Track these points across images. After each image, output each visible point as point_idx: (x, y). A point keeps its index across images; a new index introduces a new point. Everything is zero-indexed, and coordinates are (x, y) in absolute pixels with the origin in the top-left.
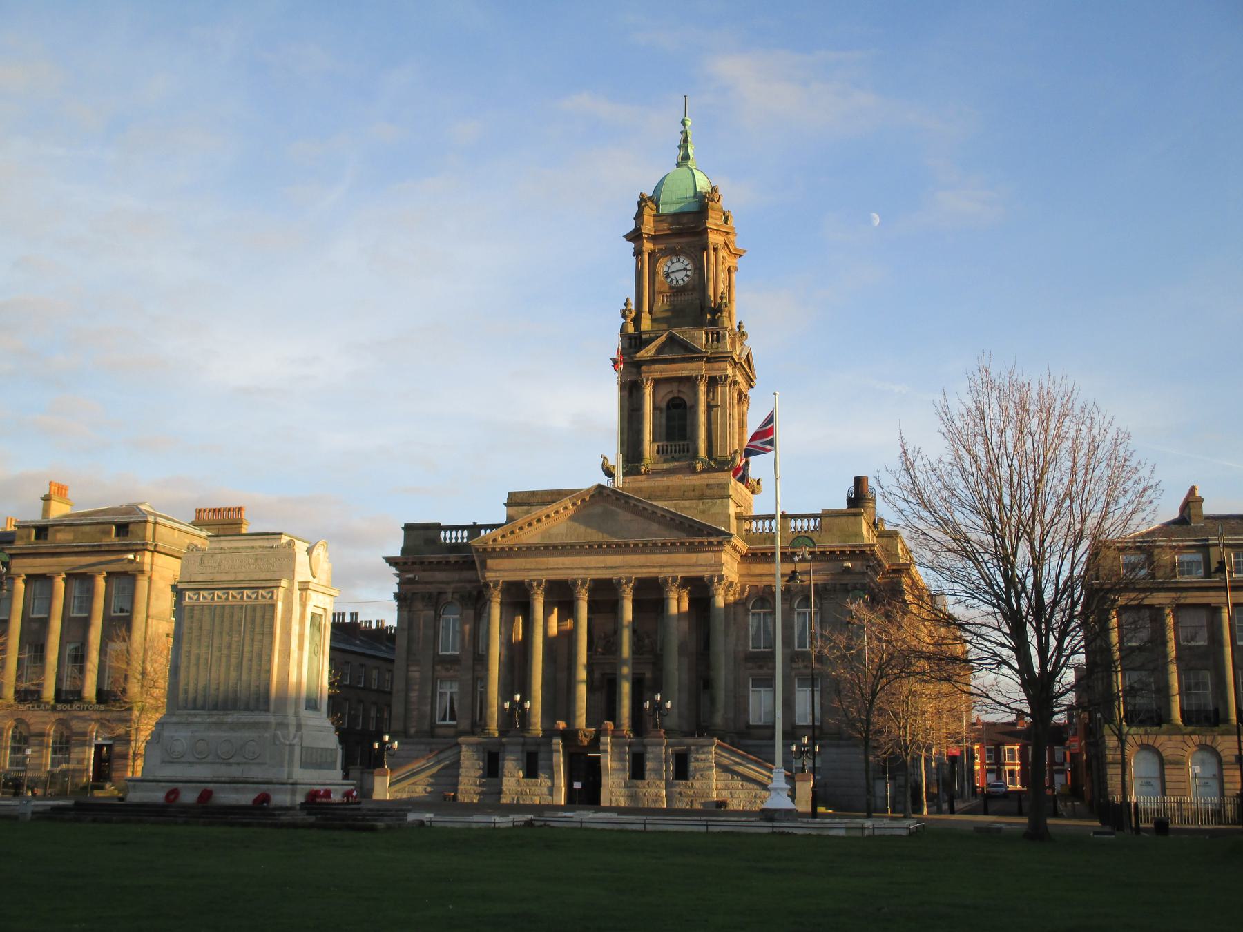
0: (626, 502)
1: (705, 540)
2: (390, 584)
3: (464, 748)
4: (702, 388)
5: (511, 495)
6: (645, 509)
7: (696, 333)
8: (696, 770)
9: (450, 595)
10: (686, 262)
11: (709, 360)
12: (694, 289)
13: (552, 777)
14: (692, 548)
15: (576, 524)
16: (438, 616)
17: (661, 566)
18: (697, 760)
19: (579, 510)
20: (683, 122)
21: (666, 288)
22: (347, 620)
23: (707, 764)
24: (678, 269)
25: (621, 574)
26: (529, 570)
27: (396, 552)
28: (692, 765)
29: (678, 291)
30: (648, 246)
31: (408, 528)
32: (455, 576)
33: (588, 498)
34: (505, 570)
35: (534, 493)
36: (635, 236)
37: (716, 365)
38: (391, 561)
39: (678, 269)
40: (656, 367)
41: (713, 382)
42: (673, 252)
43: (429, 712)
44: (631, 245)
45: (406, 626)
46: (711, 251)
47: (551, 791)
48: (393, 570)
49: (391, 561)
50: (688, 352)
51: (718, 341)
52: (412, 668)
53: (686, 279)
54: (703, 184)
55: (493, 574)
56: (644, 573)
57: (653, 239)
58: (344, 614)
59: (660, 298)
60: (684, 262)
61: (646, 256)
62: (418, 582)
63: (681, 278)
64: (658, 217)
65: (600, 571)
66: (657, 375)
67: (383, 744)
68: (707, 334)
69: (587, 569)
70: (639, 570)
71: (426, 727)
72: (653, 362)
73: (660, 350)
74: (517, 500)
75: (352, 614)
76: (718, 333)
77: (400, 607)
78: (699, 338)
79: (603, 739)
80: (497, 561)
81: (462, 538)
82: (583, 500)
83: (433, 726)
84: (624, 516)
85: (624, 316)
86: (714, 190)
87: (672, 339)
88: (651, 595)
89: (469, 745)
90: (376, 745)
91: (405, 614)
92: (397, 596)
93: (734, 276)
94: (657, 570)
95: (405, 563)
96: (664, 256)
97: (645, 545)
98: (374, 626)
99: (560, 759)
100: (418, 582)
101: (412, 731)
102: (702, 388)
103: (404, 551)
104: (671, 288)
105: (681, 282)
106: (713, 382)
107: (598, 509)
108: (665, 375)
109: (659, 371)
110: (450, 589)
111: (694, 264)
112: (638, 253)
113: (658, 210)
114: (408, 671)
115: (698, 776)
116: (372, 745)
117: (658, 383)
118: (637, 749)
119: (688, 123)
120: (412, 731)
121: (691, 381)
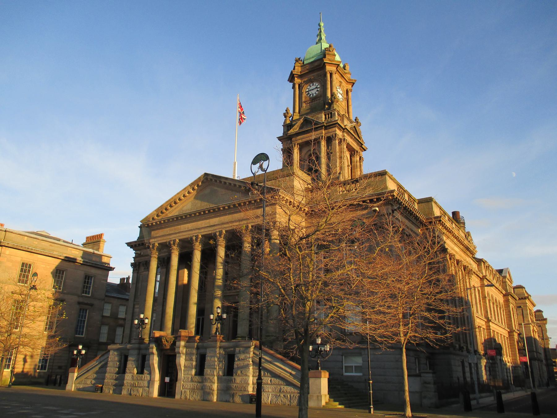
0: (220, 182)
3: (111, 352)
4: (323, 143)
6: (230, 184)
7: (319, 116)
8: (238, 368)
10: (317, 84)
11: (326, 128)
12: (321, 96)
13: (150, 374)
15: (197, 201)
18: (239, 360)
19: (198, 193)
20: (320, 26)
21: (308, 99)
23: (246, 363)
24: (313, 89)
25: (217, 229)
28: (237, 364)
29: (313, 99)
30: (297, 81)
33: (200, 184)
34: (159, 237)
36: (292, 78)
37: (330, 130)
38: (131, 245)
39: (313, 89)
40: (299, 137)
41: (329, 140)
42: (311, 81)
44: (291, 84)
45: (135, 282)
46: (329, 75)
47: (150, 383)
49: (131, 245)
50: (319, 127)
51: (331, 117)
53: (317, 92)
54: (325, 45)
56: (229, 227)
57: (300, 77)
59: (304, 105)
60: (316, 84)
61: (297, 86)
62: (142, 256)
63: (314, 93)
64: (303, 65)
65: (206, 230)
66: (300, 141)
67: (79, 351)
68: (325, 115)
69: (199, 229)
70: (227, 225)
72: (297, 134)
73: (301, 128)
76: (331, 113)
78: (322, 118)
79: (177, 343)
80: (156, 232)
82: (198, 186)
84: (221, 191)
85: (285, 117)
86: (330, 46)
87: (307, 122)
88: (234, 241)
89: (115, 350)
90: (75, 352)
91: (136, 274)
92: (132, 265)
93: (350, 94)
95: (135, 245)
96: (306, 84)
97: (229, 207)
99: (155, 360)
100: (142, 256)
102: (323, 143)
104: (310, 98)
105: (315, 95)
106: (329, 140)
107: (207, 191)
108: (304, 140)
109: (301, 139)
111: (320, 83)
112: (294, 87)
113: (303, 63)
114: (134, 308)
115: (239, 372)
116: (73, 352)
117: (302, 146)
118: (202, 351)
119: (322, 24)
121: (317, 141)
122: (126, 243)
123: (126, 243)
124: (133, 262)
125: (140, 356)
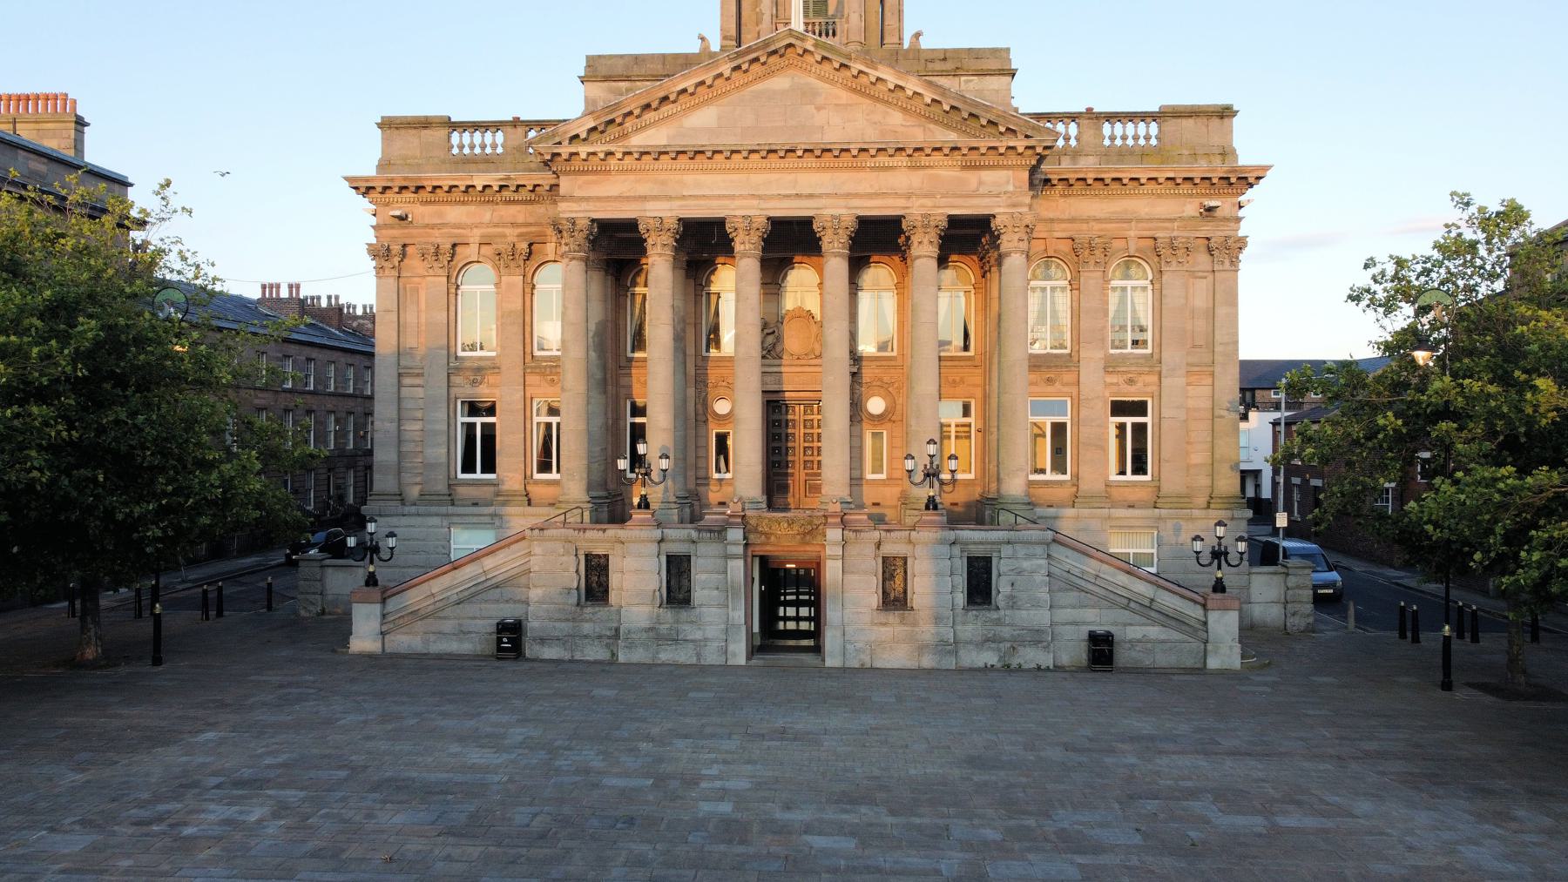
1: (1003, 143)
2: (359, 222)
5: (592, 62)
9: (474, 248)
14: (972, 160)
16: (453, 287)
17: (908, 196)
22: (284, 294)
26: (644, 198)
27: (367, 167)
31: (388, 125)
32: (486, 214)
35: (637, 59)
43: (444, 459)
48: (364, 203)
52: (407, 381)
55: (574, 206)
58: (278, 286)
71: (441, 487)
74: (598, 70)
75: (291, 286)
77: (380, 269)
81: (494, 146)
83: (452, 484)
94: (902, 202)
98: (324, 304)
101: (414, 492)
103: (383, 165)
110: (475, 236)
120: (414, 492)
122: (346, 179)
123: (346, 179)
124: (374, 241)
125: (664, 559)
